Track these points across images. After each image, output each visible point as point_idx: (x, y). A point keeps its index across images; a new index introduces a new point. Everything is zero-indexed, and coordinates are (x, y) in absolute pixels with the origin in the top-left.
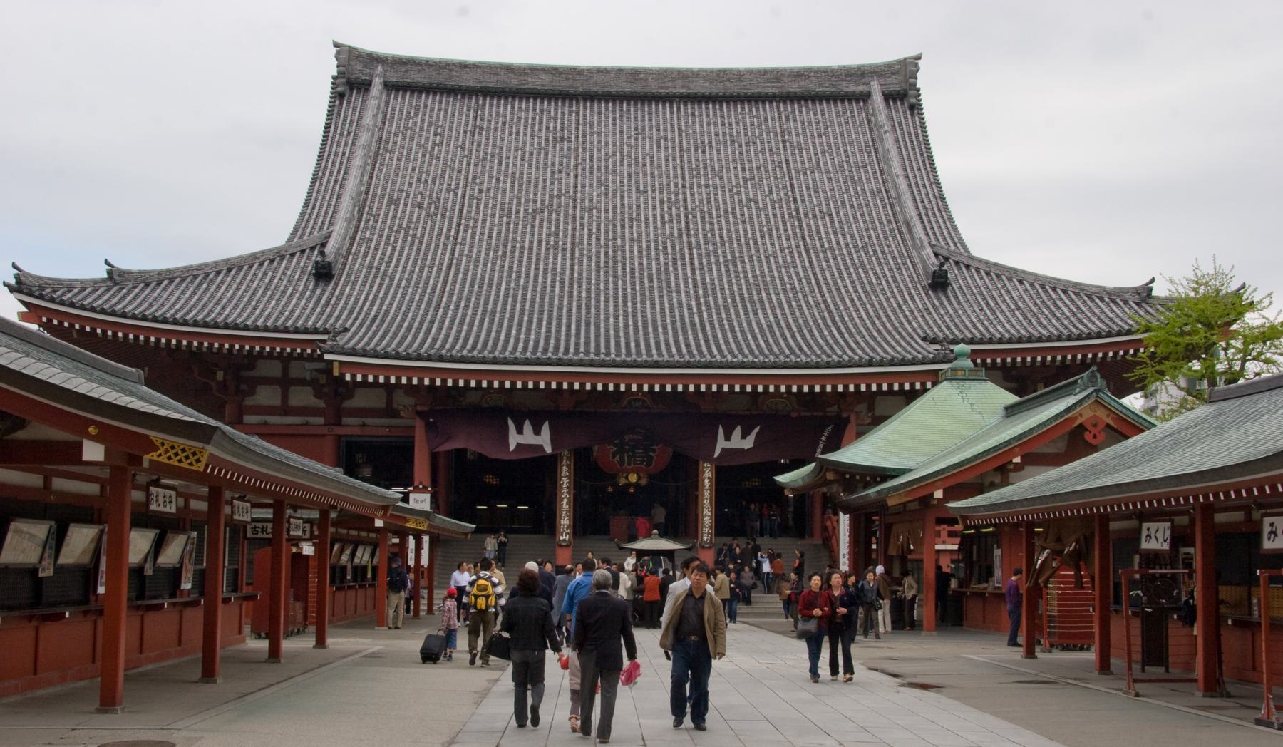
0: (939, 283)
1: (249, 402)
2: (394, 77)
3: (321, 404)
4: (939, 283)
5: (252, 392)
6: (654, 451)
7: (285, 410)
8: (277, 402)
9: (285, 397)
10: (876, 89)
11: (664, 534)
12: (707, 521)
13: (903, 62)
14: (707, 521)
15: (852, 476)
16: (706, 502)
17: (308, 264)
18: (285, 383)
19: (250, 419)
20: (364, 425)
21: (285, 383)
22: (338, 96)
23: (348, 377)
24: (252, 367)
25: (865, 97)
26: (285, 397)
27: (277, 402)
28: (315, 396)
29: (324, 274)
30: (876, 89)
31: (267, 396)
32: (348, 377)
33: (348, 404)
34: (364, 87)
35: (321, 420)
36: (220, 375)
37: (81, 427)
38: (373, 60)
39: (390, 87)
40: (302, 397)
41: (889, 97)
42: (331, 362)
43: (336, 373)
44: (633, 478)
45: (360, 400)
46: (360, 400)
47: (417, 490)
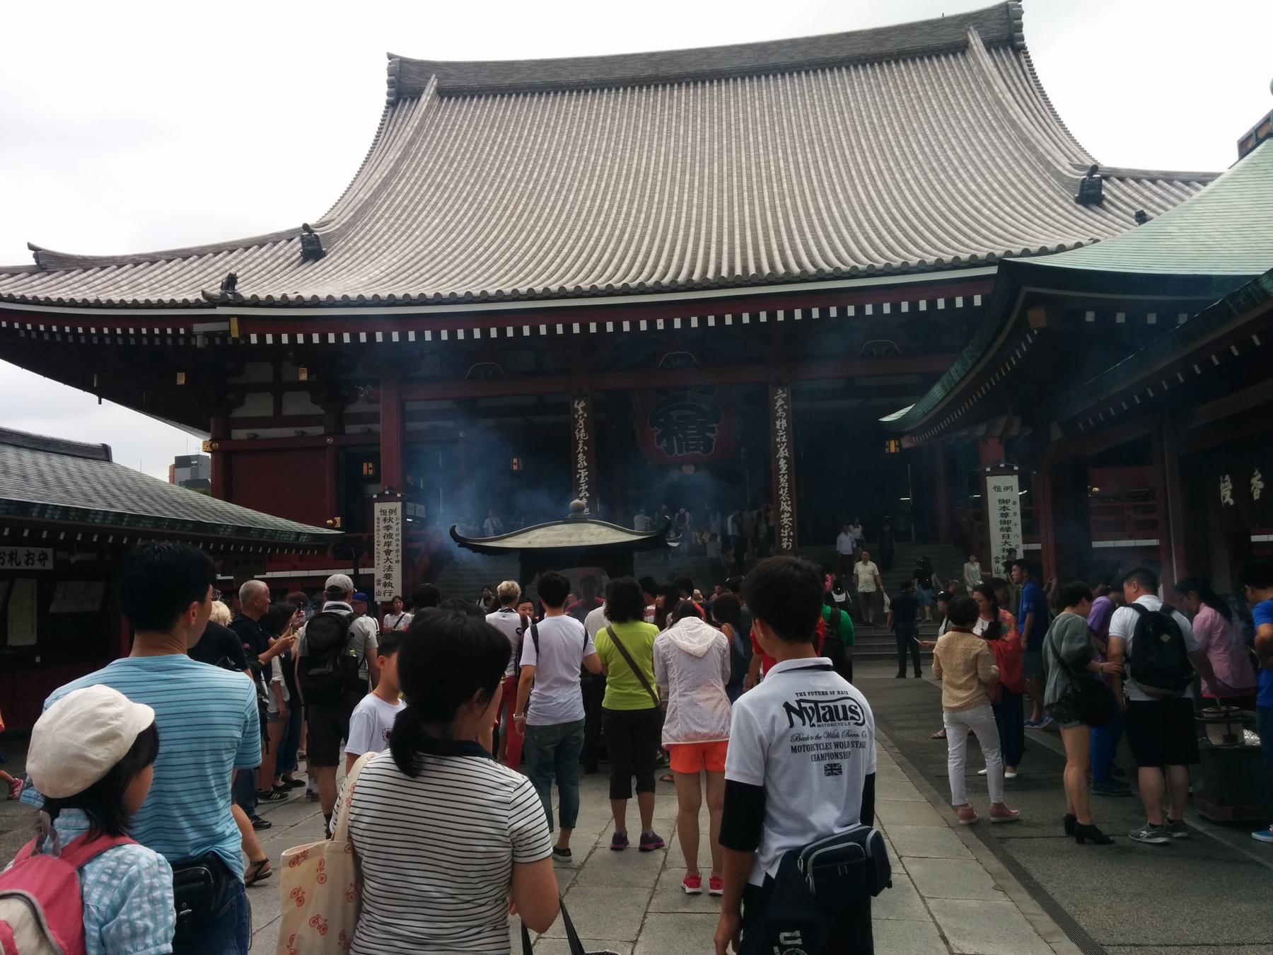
1: (239, 413)
2: (449, 83)
3: (318, 410)
5: (241, 403)
6: (712, 430)
7: (278, 419)
8: (269, 412)
9: (278, 405)
10: (976, 41)
13: (1004, 8)
15: (1104, 313)
16: (783, 493)
18: (279, 389)
19: (240, 434)
20: (370, 430)
21: (279, 389)
22: (392, 105)
23: (254, 339)
25: (961, 48)
26: (278, 405)
27: (269, 412)
28: (314, 401)
31: (258, 406)
32: (254, 339)
34: (416, 95)
35: (320, 430)
36: (181, 379)
38: (427, 68)
39: (442, 93)
40: (297, 404)
41: (990, 45)
42: (227, 318)
43: (235, 334)
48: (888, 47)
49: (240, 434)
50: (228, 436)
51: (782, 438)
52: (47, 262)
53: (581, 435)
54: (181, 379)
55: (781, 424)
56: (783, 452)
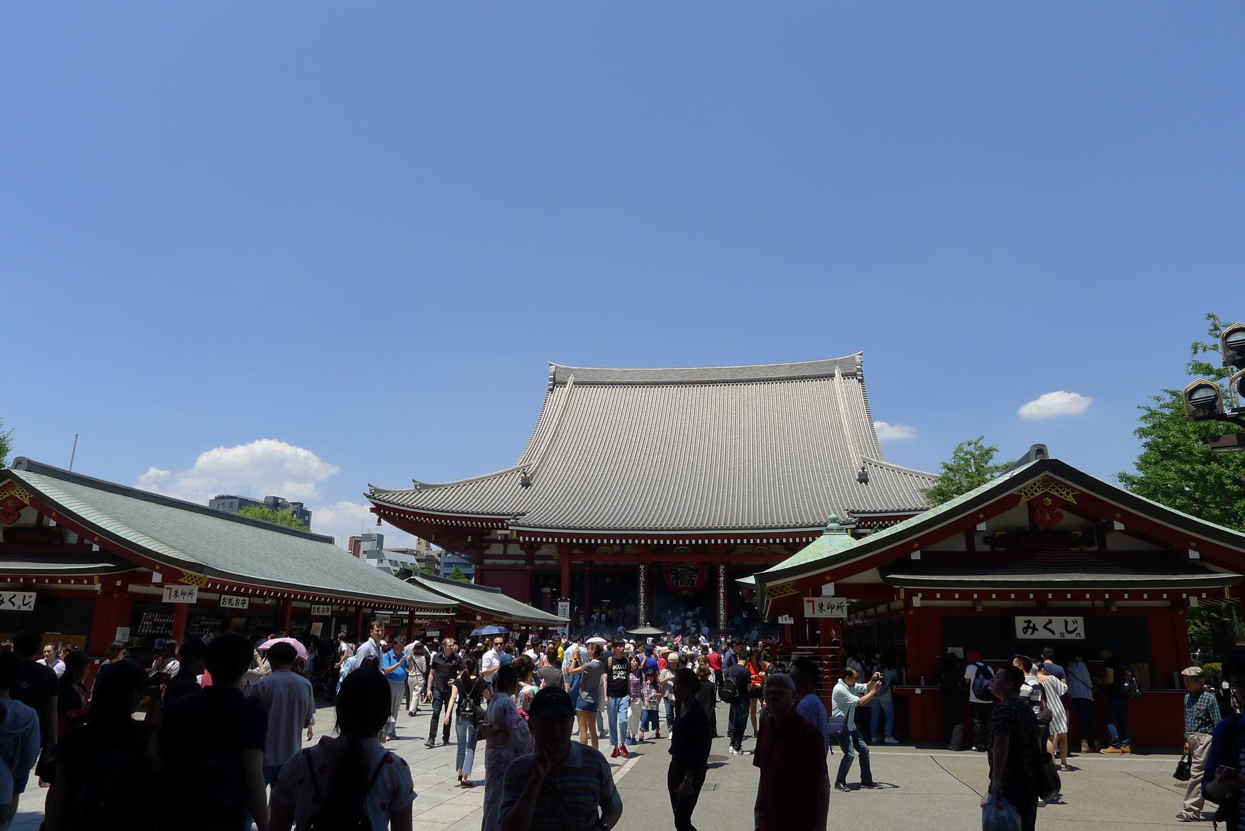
0: (863, 479)
1: (487, 552)
3: (523, 553)
4: (863, 479)
5: (489, 548)
9: (505, 550)
11: (652, 626)
12: (722, 617)
14: (722, 617)
17: (518, 478)
19: (487, 562)
24: (489, 534)
25: (832, 376)
26: (505, 550)
29: (526, 483)
30: (837, 372)
31: (496, 549)
33: (538, 553)
35: (523, 562)
36: (469, 539)
37: (152, 565)
40: (514, 549)
44: (685, 592)
45: (544, 551)
46: (544, 551)
47: (562, 600)
48: (796, 374)
49: (487, 562)
50: (482, 563)
51: (722, 584)
52: (421, 487)
53: (642, 579)
54: (469, 539)
55: (722, 579)
56: (722, 590)
